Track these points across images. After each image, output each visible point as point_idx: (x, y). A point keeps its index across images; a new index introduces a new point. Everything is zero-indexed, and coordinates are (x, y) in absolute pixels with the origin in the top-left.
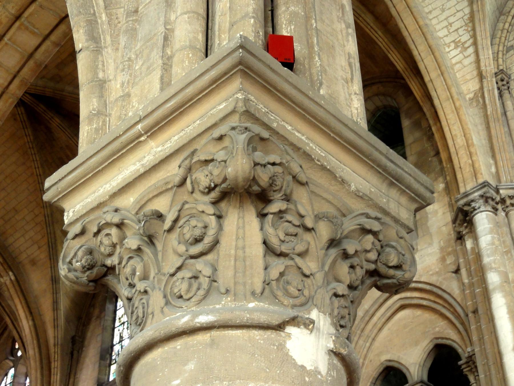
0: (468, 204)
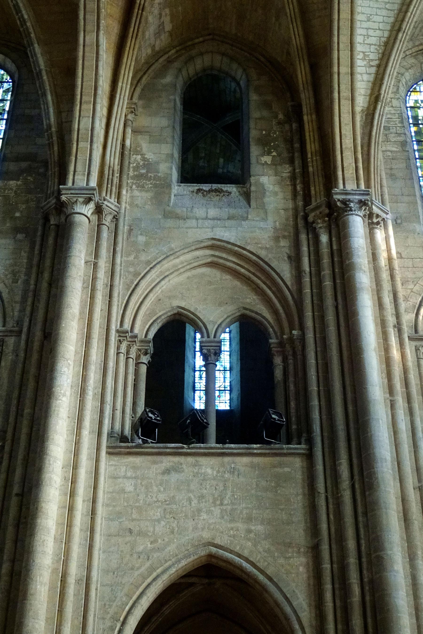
0: (345, 202)
